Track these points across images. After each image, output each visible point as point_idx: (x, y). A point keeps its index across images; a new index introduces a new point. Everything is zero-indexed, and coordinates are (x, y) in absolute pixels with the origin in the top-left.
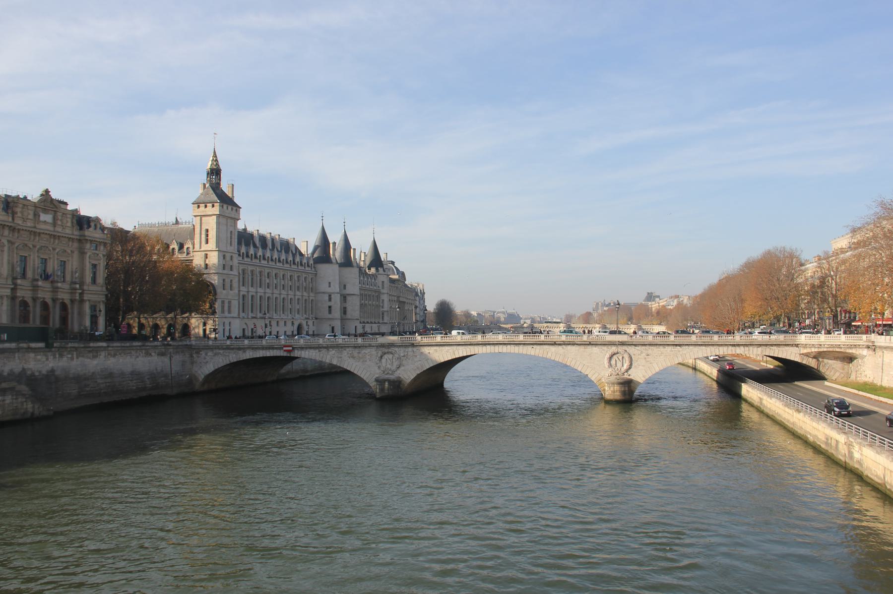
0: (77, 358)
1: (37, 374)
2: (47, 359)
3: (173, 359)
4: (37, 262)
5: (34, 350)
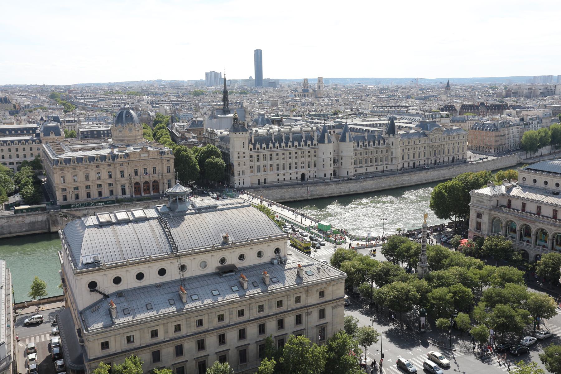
4: (143, 170)
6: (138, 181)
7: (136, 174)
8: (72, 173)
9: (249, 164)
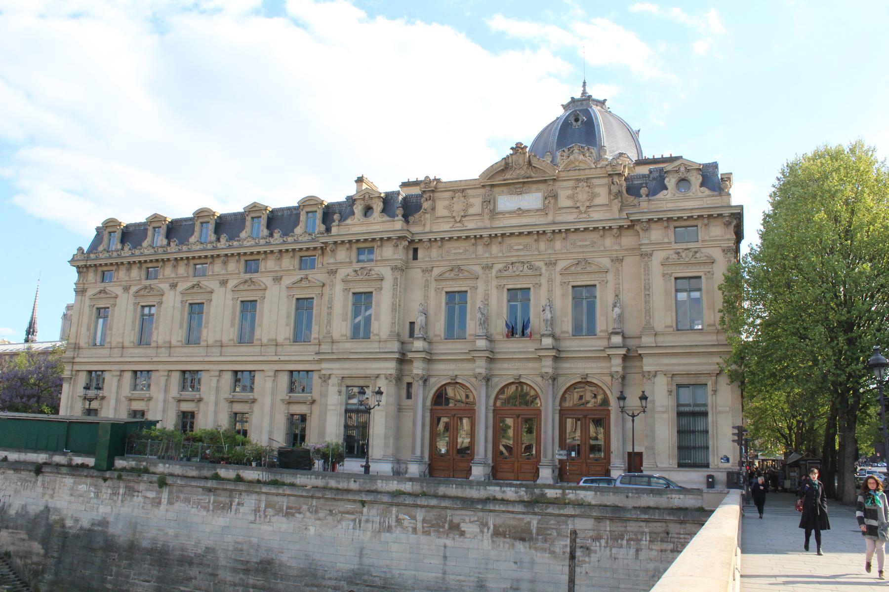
0: (170, 503)
1: (69, 523)
2: (97, 496)
5: (75, 470)
7: (455, 327)
8: (137, 294)
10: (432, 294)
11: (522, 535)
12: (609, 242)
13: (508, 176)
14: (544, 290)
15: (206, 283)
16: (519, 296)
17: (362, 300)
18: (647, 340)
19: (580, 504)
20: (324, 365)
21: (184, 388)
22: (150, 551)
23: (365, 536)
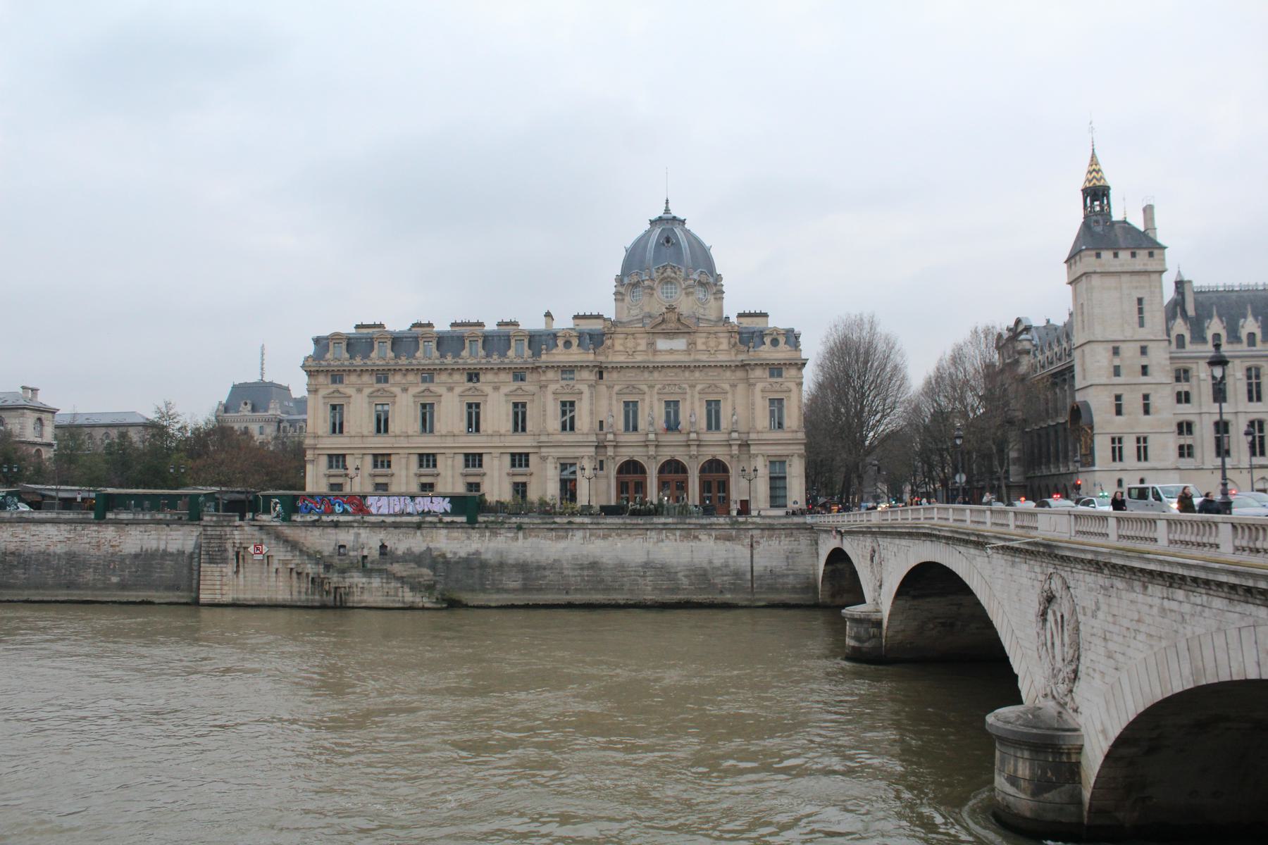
0: (525, 538)
1: (449, 555)
3: (759, 550)
6: (638, 454)
7: (631, 425)
8: (370, 396)
9: (1167, 410)
10: (614, 402)
11: (729, 538)
12: (728, 374)
13: (663, 326)
14: (688, 402)
15: (433, 387)
16: (672, 407)
17: (567, 407)
18: (753, 436)
19: (753, 523)
20: (543, 450)
21: (421, 466)
22: (513, 566)
23: (649, 545)
